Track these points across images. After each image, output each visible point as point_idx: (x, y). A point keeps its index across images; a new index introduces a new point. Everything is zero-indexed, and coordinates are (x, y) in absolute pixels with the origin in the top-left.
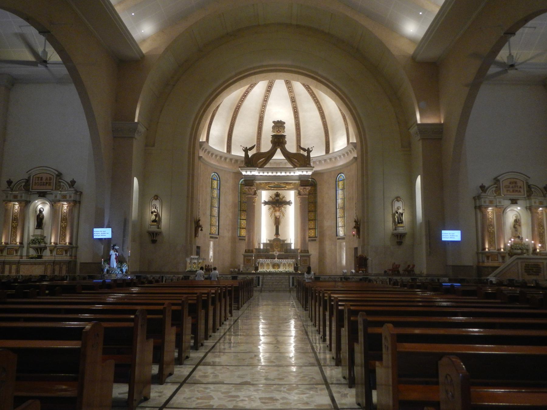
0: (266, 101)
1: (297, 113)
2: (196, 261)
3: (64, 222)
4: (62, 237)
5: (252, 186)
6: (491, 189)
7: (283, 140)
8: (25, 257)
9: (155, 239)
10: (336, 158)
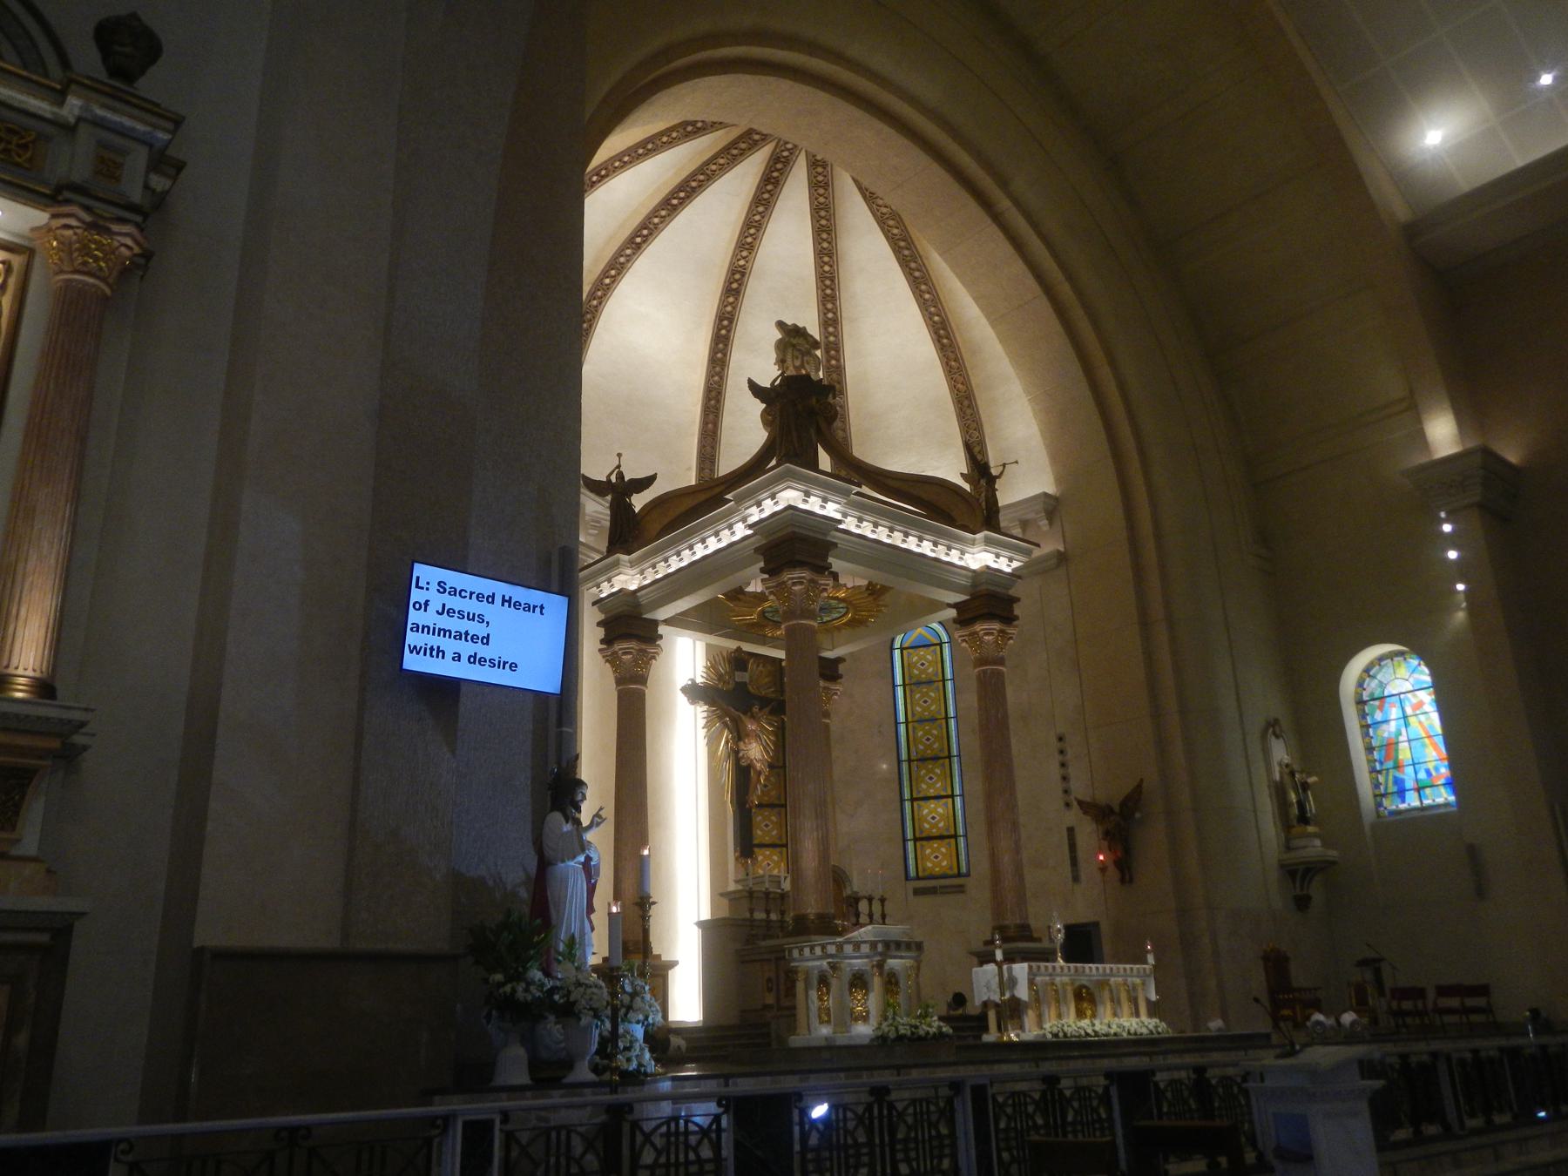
0: (638, 248)
1: (726, 345)
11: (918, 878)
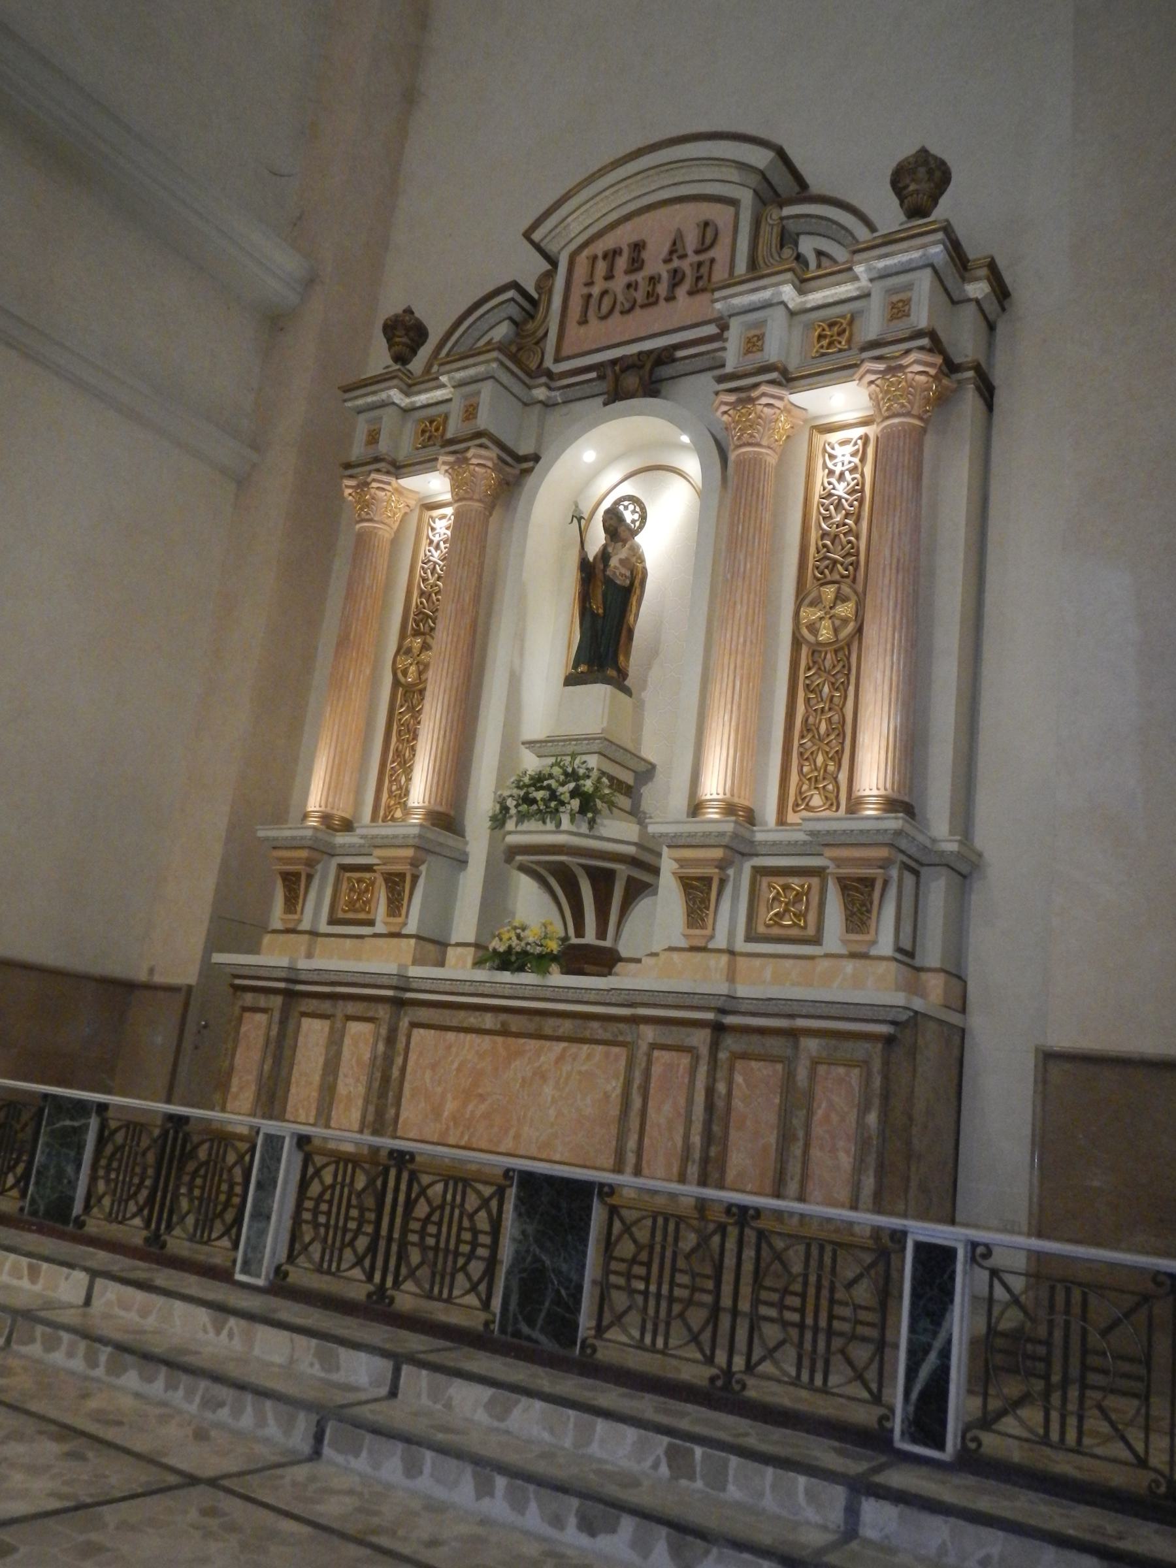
3: (829, 592)
4: (811, 759)
8: (469, 954)
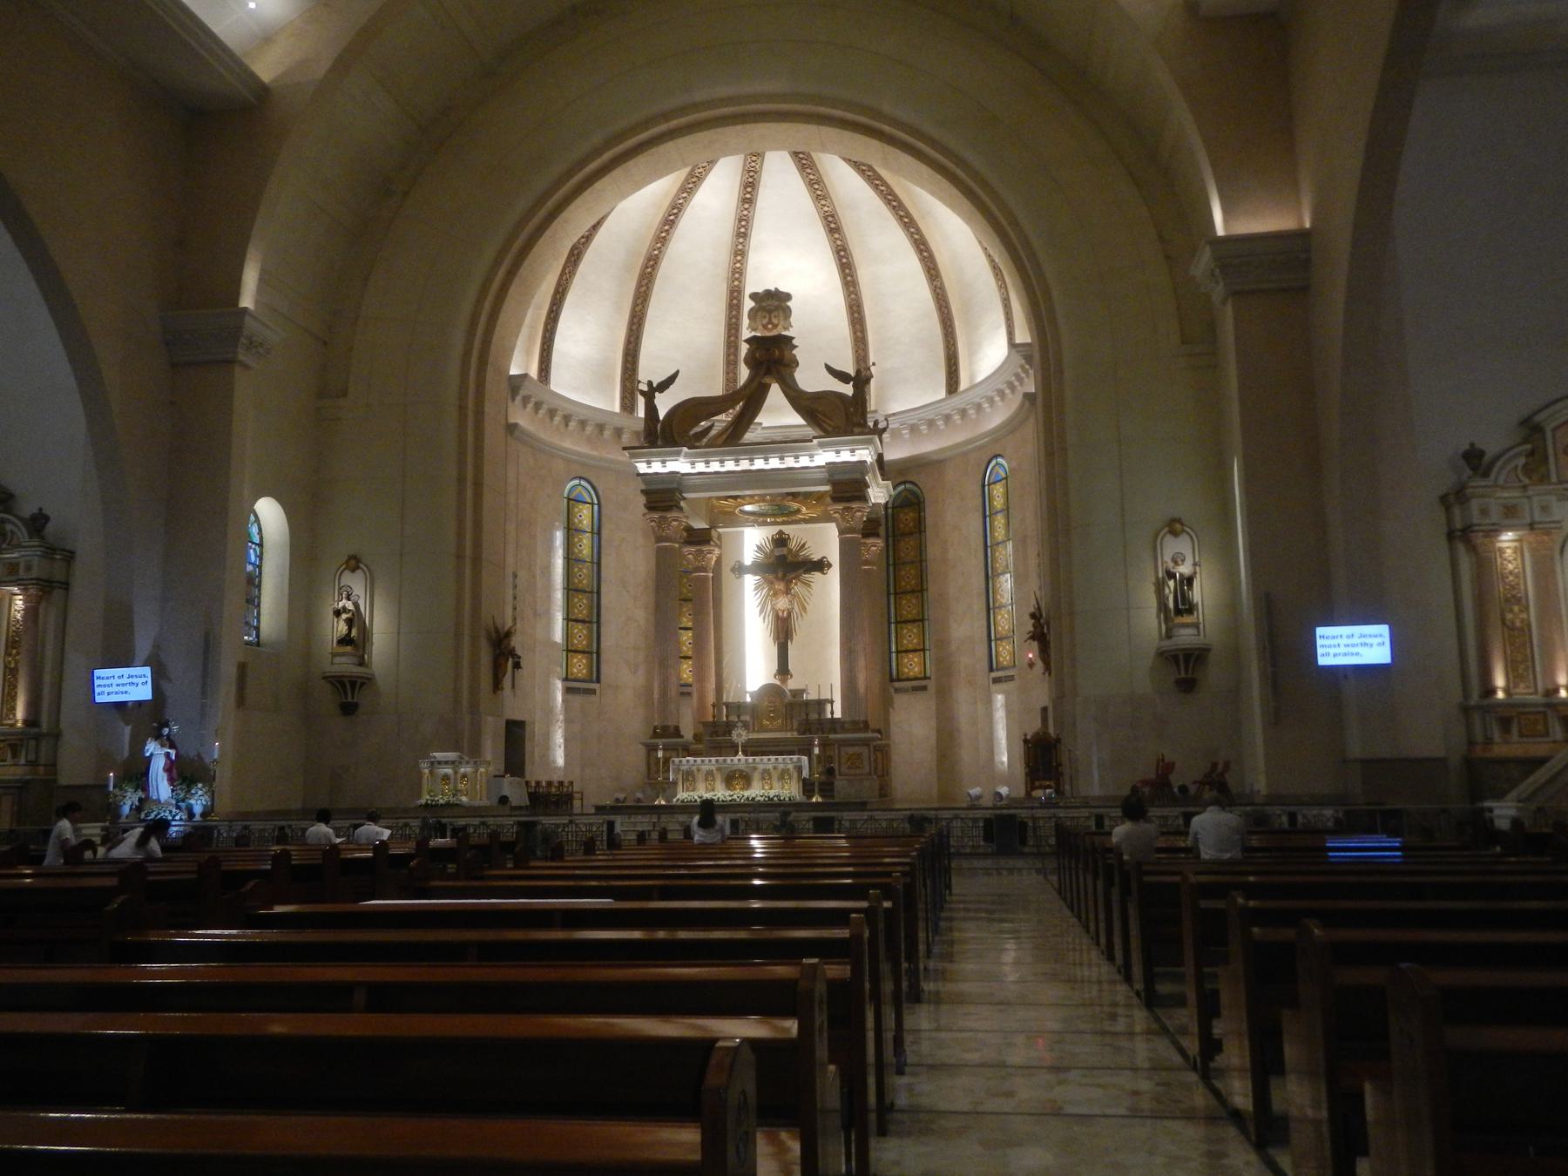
1: (850, 269)
2: (449, 771)
5: (669, 509)
6: (1510, 459)
7: (781, 351)
9: (350, 699)
10: (979, 407)
11: (998, 670)
